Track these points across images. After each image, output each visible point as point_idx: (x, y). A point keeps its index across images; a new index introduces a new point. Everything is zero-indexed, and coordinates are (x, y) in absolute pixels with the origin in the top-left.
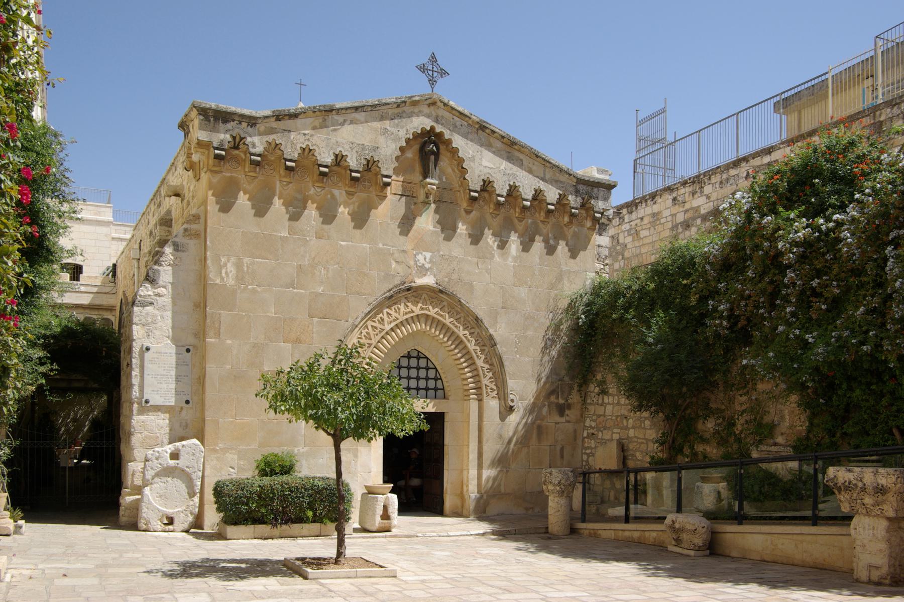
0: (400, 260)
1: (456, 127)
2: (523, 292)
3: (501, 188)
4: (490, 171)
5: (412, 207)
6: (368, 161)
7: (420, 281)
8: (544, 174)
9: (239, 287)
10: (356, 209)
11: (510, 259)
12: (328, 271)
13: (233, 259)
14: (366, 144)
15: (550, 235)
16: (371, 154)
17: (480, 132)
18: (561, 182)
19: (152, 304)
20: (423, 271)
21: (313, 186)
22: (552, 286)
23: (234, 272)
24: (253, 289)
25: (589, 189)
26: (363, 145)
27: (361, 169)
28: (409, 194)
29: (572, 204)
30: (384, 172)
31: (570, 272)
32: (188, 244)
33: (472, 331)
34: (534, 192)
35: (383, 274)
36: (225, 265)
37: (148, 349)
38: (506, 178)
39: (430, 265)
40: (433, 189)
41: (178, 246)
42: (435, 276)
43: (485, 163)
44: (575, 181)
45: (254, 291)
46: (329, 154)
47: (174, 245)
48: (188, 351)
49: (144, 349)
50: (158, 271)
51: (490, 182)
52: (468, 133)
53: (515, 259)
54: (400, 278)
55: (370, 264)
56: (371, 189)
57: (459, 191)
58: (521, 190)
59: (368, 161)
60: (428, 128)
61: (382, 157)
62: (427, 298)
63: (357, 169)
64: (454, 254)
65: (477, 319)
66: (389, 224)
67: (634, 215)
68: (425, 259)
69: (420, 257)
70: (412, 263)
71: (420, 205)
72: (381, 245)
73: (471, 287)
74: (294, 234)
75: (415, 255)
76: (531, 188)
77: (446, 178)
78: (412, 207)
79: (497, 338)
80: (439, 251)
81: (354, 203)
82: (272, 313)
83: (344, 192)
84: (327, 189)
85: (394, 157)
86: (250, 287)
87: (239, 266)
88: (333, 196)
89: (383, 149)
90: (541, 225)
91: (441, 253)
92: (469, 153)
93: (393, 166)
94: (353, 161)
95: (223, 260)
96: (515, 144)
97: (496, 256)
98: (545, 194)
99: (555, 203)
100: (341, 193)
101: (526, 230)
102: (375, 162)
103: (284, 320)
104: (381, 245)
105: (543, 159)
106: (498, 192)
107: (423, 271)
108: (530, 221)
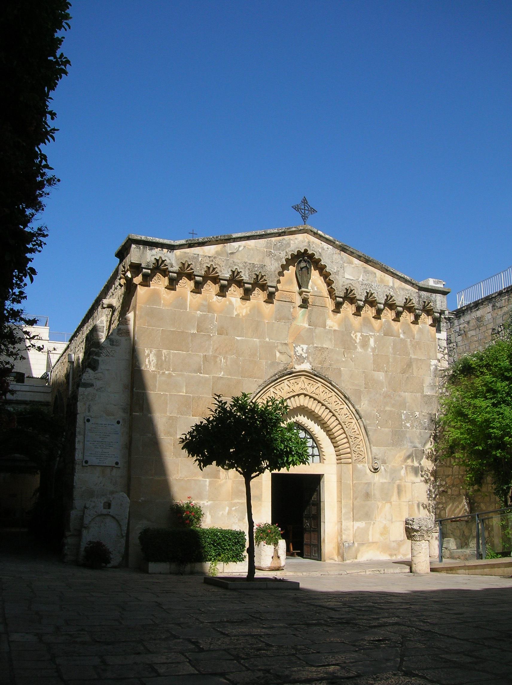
1: (324, 249)
2: (381, 376)
3: (360, 295)
5: (292, 310)
6: (257, 276)
7: (298, 368)
8: (393, 284)
9: (159, 372)
11: (370, 350)
12: (227, 360)
13: (154, 351)
15: (400, 331)
16: (259, 271)
17: (342, 253)
18: (407, 290)
19: (92, 385)
20: (301, 359)
22: (404, 372)
23: (155, 361)
24: (169, 373)
25: (428, 294)
27: (252, 282)
29: (416, 306)
30: (269, 284)
31: (417, 360)
32: (120, 340)
33: (342, 406)
34: (386, 298)
36: (148, 355)
37: (88, 420)
39: (306, 355)
40: (308, 295)
41: (113, 342)
43: (347, 276)
44: (418, 288)
45: (170, 375)
46: (228, 271)
47: (110, 341)
48: (118, 422)
49: (86, 421)
50: (98, 361)
52: (333, 254)
53: (374, 349)
54: (283, 365)
55: (260, 354)
59: (257, 276)
60: (303, 251)
62: (305, 380)
63: (249, 282)
64: (325, 346)
65: (345, 396)
67: (461, 320)
68: (303, 350)
69: (298, 349)
70: (292, 353)
71: (298, 309)
72: (267, 339)
73: (339, 372)
74: (202, 331)
78: (292, 310)
79: (362, 413)
80: (313, 344)
81: (247, 307)
82: (183, 392)
83: (239, 299)
85: (277, 273)
86: (167, 372)
87: (158, 356)
88: (231, 303)
91: (315, 345)
92: (334, 269)
94: (245, 276)
95: (147, 352)
96: (370, 261)
97: (358, 347)
99: (403, 305)
100: (236, 301)
101: (381, 326)
102: (262, 276)
103: (193, 398)
104: (267, 339)
105: (391, 272)
106: (358, 297)
107: (301, 359)
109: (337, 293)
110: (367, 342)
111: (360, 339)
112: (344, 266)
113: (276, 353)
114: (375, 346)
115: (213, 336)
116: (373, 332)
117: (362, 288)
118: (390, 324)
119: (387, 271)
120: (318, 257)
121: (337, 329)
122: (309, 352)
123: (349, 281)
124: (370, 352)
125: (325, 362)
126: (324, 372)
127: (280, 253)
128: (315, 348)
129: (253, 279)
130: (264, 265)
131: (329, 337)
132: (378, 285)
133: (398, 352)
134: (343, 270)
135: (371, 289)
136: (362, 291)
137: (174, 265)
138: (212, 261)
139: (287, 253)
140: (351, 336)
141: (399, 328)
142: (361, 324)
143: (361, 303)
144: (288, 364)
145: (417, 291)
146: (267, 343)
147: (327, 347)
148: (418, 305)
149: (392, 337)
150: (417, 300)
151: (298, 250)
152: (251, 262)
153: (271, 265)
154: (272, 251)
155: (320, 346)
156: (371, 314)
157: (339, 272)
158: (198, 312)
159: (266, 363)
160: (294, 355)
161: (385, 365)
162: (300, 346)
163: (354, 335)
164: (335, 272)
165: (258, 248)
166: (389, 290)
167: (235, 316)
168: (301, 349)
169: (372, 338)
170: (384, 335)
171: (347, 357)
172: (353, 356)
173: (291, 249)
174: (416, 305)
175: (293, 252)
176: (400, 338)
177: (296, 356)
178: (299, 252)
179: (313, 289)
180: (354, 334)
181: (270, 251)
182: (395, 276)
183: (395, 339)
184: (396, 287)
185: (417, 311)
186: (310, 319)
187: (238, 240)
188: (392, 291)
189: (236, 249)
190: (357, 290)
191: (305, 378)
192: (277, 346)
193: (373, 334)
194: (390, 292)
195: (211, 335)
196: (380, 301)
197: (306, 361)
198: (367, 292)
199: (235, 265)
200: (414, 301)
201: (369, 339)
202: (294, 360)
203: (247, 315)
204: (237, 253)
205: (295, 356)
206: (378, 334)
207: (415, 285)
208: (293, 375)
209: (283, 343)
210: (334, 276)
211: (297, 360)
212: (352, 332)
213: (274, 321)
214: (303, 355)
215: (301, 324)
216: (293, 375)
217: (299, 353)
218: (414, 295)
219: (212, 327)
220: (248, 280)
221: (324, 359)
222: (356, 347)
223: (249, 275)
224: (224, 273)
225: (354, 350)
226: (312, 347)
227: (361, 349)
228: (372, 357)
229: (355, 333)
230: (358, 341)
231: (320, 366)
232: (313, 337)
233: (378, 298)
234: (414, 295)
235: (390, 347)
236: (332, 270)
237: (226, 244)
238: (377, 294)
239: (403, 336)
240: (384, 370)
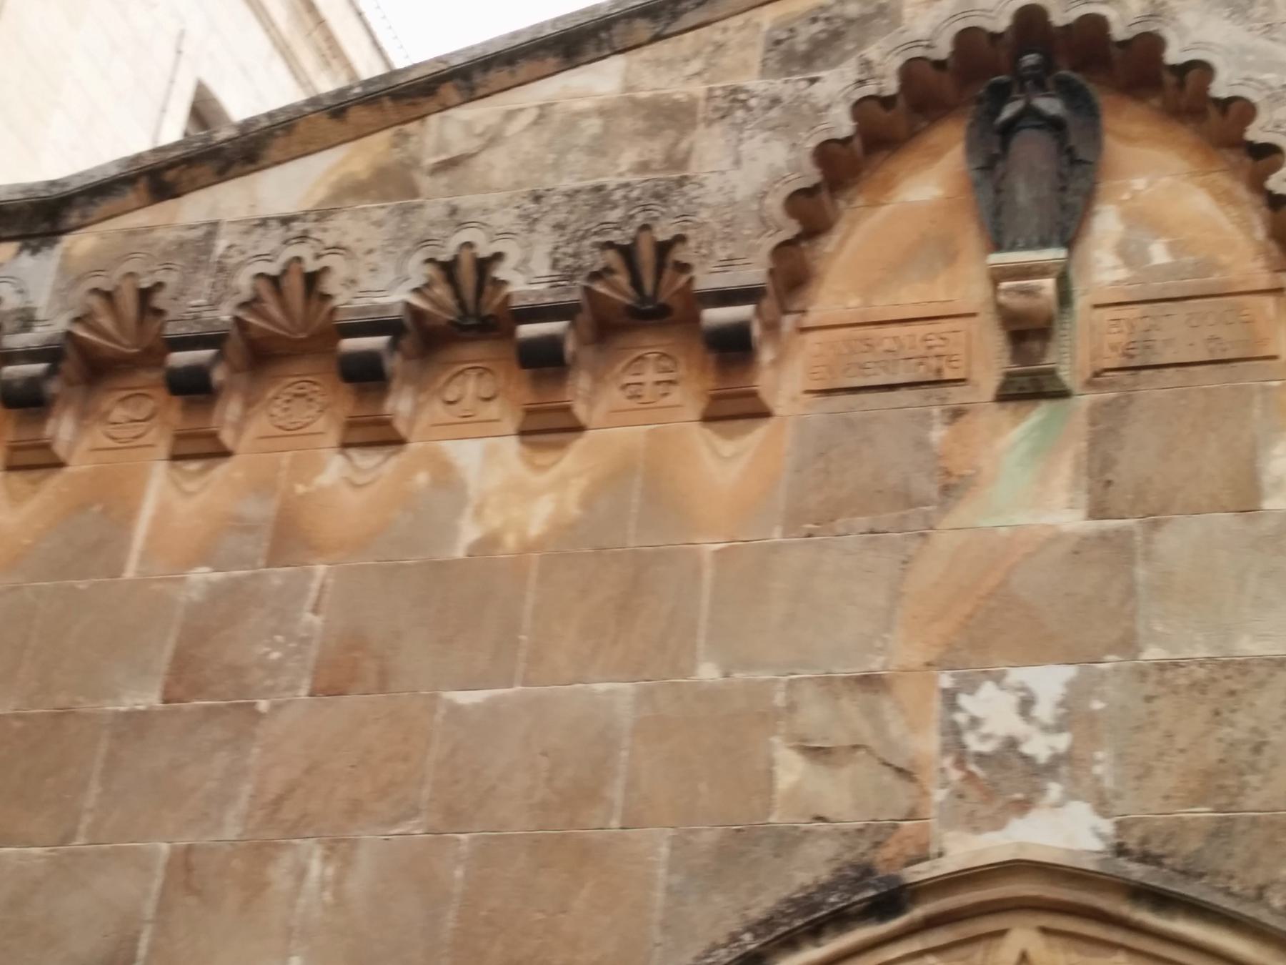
0: (840, 738)
5: (938, 434)
10: (574, 511)
12: (347, 862)
14: (611, 181)
21: (345, 446)
26: (598, 189)
28: (921, 374)
30: (706, 280)
35: (708, 836)
39: (1062, 742)
42: (1102, 806)
46: (400, 268)
55: (631, 786)
56: (676, 395)
59: (628, 253)
61: (704, 215)
64: (1248, 646)
66: (776, 548)
68: (1026, 705)
70: (928, 743)
75: (950, 699)
77: (1173, 248)
80: (1128, 645)
83: (511, 445)
84: (414, 446)
85: (775, 204)
88: (446, 476)
89: (712, 183)
91: (1153, 653)
93: (770, 242)
102: (663, 249)
104: (708, 672)
113: (771, 762)
115: (276, 707)
120: (1139, 29)
122: (1092, 718)
126: (1252, 863)
127: (813, 81)
128: (1154, 676)
129: (581, 281)
130: (681, 182)
137: (40, 315)
138: (303, 237)
139: (867, 65)
144: (878, 834)
146: (708, 694)
151: (960, 25)
152: (577, 185)
153: (737, 163)
154: (754, 83)
155: (1201, 653)
158: (201, 575)
159: (679, 844)
160: (945, 751)
162: (998, 679)
165: (643, 95)
167: (460, 553)
168: (1012, 700)
173: (908, 37)
175: (918, 52)
177: (960, 763)
178: (968, 39)
179: (1129, 254)
181: (735, 90)
186: (1107, 463)
187: (498, 76)
189: (481, 135)
191: (1045, 931)
192: (792, 708)
195: (263, 705)
197: (1055, 790)
199: (461, 225)
202: (939, 795)
203: (561, 530)
204: (484, 157)
205: (948, 762)
208: (918, 912)
209: (846, 680)
211: (973, 794)
213: (777, 536)
214: (1026, 749)
215: (1021, 519)
216: (918, 912)
217: (986, 737)
219: (275, 655)
220: (541, 294)
221: (1244, 754)
223: (555, 264)
224: (376, 285)
226: (1116, 670)
231: (1203, 812)
232: (1130, 592)
236: (1266, 76)
237: (411, 127)
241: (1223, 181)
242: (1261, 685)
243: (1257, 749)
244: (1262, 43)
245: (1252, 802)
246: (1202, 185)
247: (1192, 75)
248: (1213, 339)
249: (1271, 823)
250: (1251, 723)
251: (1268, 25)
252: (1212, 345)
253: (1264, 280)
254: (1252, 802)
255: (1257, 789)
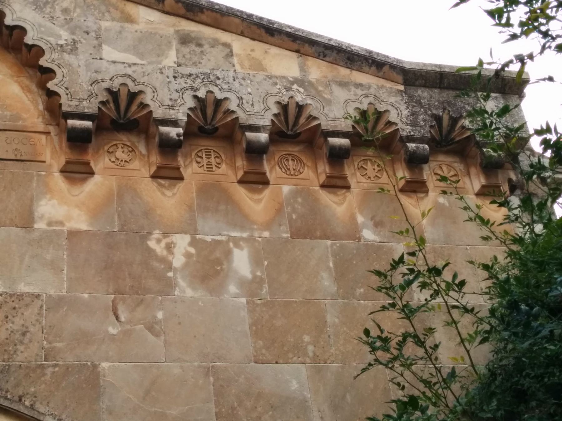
4: (129, 71)
8: (303, 68)
11: (233, 289)
15: (360, 219)
18: (359, 86)
29: (406, 130)
34: (275, 110)
38: (182, 83)
44: (400, 78)
51: (133, 96)
57: (48, 133)
58: (233, 105)
64: (23, 288)
76: (265, 101)
90: (326, 197)
92: (60, 37)
97: (182, 283)
98: (315, 113)
101: (279, 211)
106: (158, 113)
108: (286, 189)
109: (67, 105)
110: (221, 264)
111: (188, 255)
112: (99, 29)
114: (259, 274)
116: (242, 228)
117: (175, 85)
118: (316, 200)
119: (272, 35)
121: (83, 226)
123: (121, 70)
124: (237, 296)
125: (21, 348)
126: (17, 385)
131: (49, 257)
132: (240, 76)
133: (360, 288)
134: (97, 38)
135: (215, 90)
136: (175, 96)
140: (150, 251)
141: (357, 211)
142: (190, 208)
143: (173, 132)
145: (402, 88)
147: (37, 291)
148: (410, 128)
149: (329, 242)
150: (406, 112)
156: (230, 173)
157: (79, 45)
161: (307, 338)
163: (163, 244)
164: (61, 46)
166: (288, 89)
169: (242, 249)
170: (291, 237)
171: (129, 322)
172: (160, 315)
174: (404, 127)
176: (362, 242)
180: (159, 241)
182: (307, 48)
183: (342, 246)
184: (313, 81)
185: (412, 146)
188: (301, 90)
190: (155, 90)
193: (245, 235)
194: (291, 93)
196: (253, 121)
198: (195, 97)
200: (393, 117)
201: (228, 254)
206: (266, 234)
207: (386, 69)
210: (55, 56)
212: (150, 233)
218: (392, 100)
221: (18, 336)
222: (171, 285)
225: (161, 293)
227: (194, 289)
228: (244, 313)
229: (166, 235)
230: (178, 261)
233: (245, 111)
234: (392, 100)
235: (324, 275)
236: (49, 39)
238: (238, 101)
239: (374, 233)
240: (306, 354)
241: (27, 82)
242: (27, 305)
243: (24, 334)
244: (49, 24)
245: (20, 357)
246: (16, 81)
247: (16, 32)
248: (16, 150)
249: (27, 367)
250: (22, 322)
251: (51, 17)
252: (16, 153)
253: (41, 127)
254: (20, 357)
255: (22, 352)
